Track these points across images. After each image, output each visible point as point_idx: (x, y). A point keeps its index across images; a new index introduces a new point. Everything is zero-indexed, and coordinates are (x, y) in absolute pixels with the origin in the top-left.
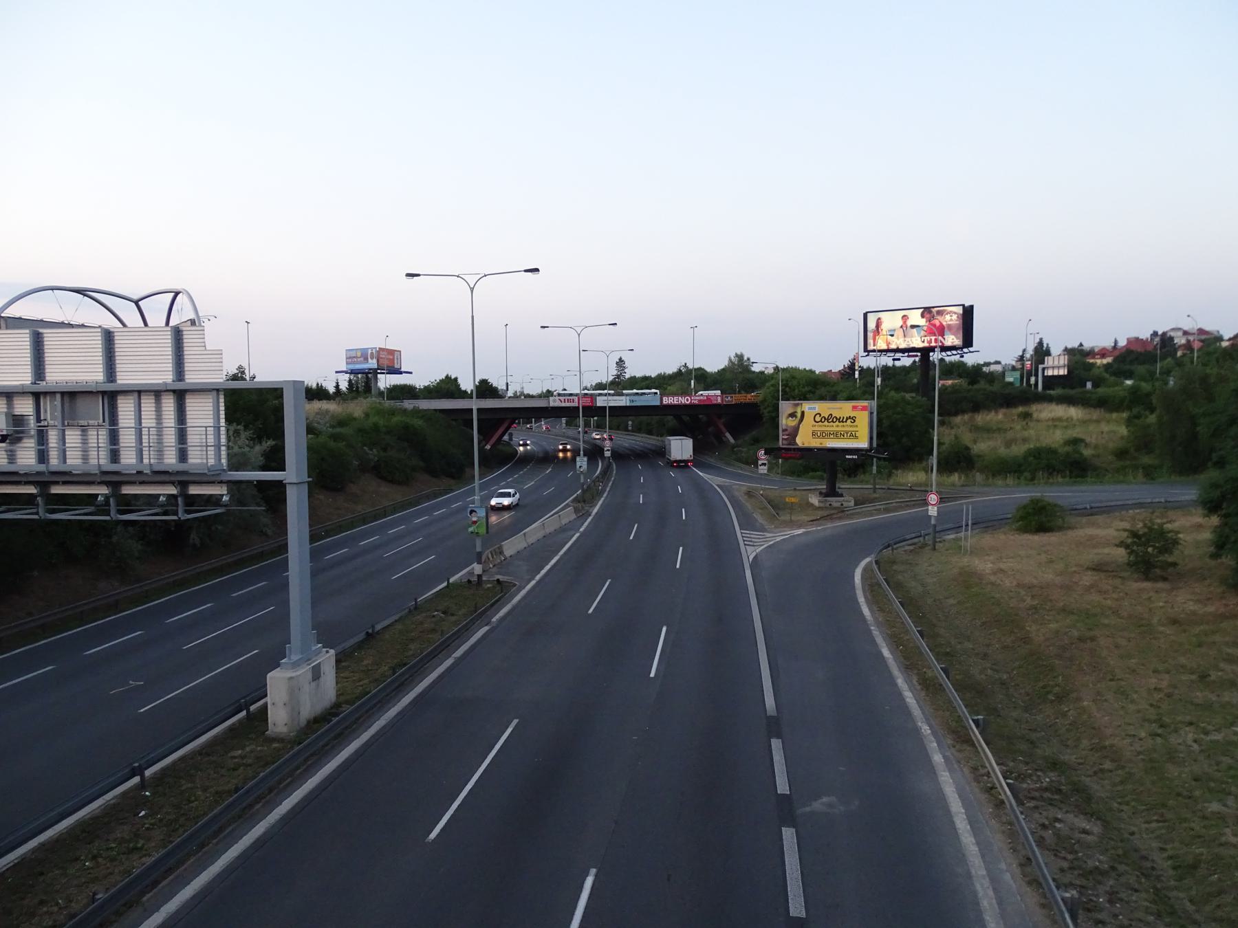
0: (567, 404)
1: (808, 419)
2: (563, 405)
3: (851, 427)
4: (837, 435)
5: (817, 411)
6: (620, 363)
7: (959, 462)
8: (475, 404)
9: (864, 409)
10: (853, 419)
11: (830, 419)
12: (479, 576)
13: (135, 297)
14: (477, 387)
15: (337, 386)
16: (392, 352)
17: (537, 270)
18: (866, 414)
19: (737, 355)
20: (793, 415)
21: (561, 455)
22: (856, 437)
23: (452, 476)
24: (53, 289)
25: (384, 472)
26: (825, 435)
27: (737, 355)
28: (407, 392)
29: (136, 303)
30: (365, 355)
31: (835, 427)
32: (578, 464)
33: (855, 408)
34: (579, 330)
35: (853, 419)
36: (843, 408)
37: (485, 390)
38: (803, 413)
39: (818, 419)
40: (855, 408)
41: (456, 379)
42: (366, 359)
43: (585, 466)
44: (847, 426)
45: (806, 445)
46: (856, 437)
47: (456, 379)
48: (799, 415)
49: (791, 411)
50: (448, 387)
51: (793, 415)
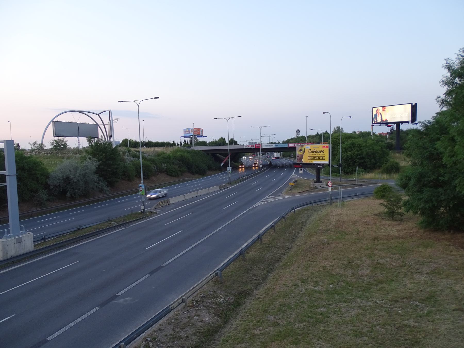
0: (251, 147)
1: (307, 152)
2: (249, 148)
3: (323, 155)
4: (317, 158)
5: (310, 148)
6: (298, 131)
7: (393, 169)
8: (229, 147)
9: (327, 147)
10: (323, 151)
11: (314, 152)
12: (144, 210)
13: (98, 113)
14: (229, 141)
15: (181, 142)
16: (199, 129)
17: (158, 98)
18: (328, 149)
19: (337, 127)
20: (301, 150)
21: (254, 168)
22: (324, 159)
23: (200, 174)
24: (71, 111)
25: (169, 173)
26: (313, 158)
27: (337, 127)
28: (204, 144)
29: (98, 115)
30: (189, 131)
31: (316, 155)
32: (228, 170)
33: (323, 147)
34: (228, 119)
35: (323, 151)
36: (319, 147)
37: (232, 142)
38: (305, 149)
39: (310, 152)
40: (323, 147)
41: (224, 139)
42: (190, 132)
43: (230, 171)
44: (321, 155)
45: (306, 162)
46: (324, 159)
47: (224, 139)
48: (303, 150)
49: (300, 149)
50: (222, 142)
51: (301, 150)
